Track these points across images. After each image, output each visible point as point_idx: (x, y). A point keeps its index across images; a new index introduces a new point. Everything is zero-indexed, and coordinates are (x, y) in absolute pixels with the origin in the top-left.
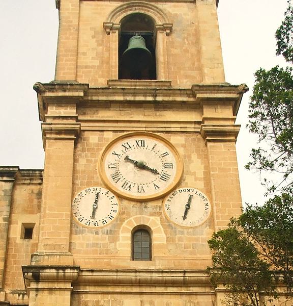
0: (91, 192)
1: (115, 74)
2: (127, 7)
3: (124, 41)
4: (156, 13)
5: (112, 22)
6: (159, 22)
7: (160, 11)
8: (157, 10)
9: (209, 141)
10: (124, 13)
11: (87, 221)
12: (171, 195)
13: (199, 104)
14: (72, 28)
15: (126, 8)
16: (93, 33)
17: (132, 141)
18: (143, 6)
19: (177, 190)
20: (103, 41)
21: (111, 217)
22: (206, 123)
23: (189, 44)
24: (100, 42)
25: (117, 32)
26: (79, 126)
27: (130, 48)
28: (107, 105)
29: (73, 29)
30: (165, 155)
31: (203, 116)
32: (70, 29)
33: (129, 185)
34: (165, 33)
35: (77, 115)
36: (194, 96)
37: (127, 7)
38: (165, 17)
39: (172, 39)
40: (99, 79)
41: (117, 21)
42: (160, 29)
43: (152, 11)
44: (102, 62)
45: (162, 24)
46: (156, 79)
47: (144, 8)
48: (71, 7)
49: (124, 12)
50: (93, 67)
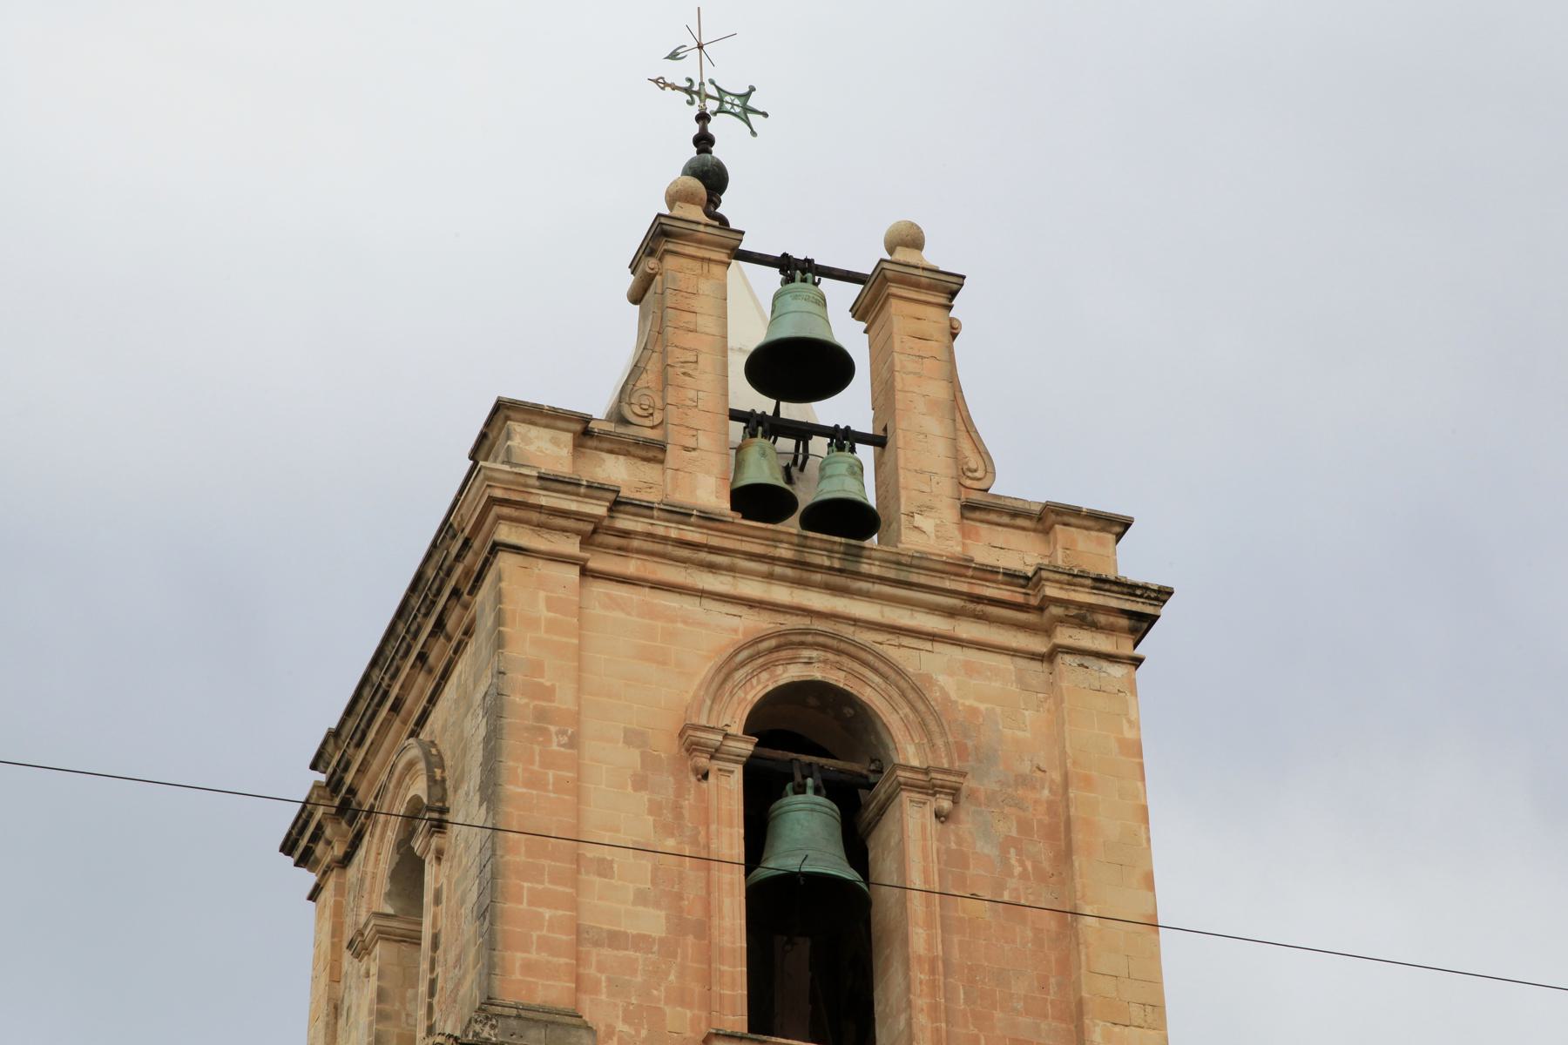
2: (778, 648)
4: (895, 694)
6: (908, 751)
8: (902, 683)
10: (764, 676)
14: (553, 729)
15: (771, 651)
16: (633, 757)
18: (839, 652)
20: (677, 809)
23: (1024, 876)
24: (668, 816)
25: (738, 771)
29: (564, 733)
32: (544, 732)
34: (929, 811)
37: (778, 648)
38: (933, 726)
39: (960, 841)
40: (668, 1010)
43: (877, 679)
44: (679, 925)
47: (844, 660)
48: (544, 613)
49: (764, 668)
50: (641, 942)
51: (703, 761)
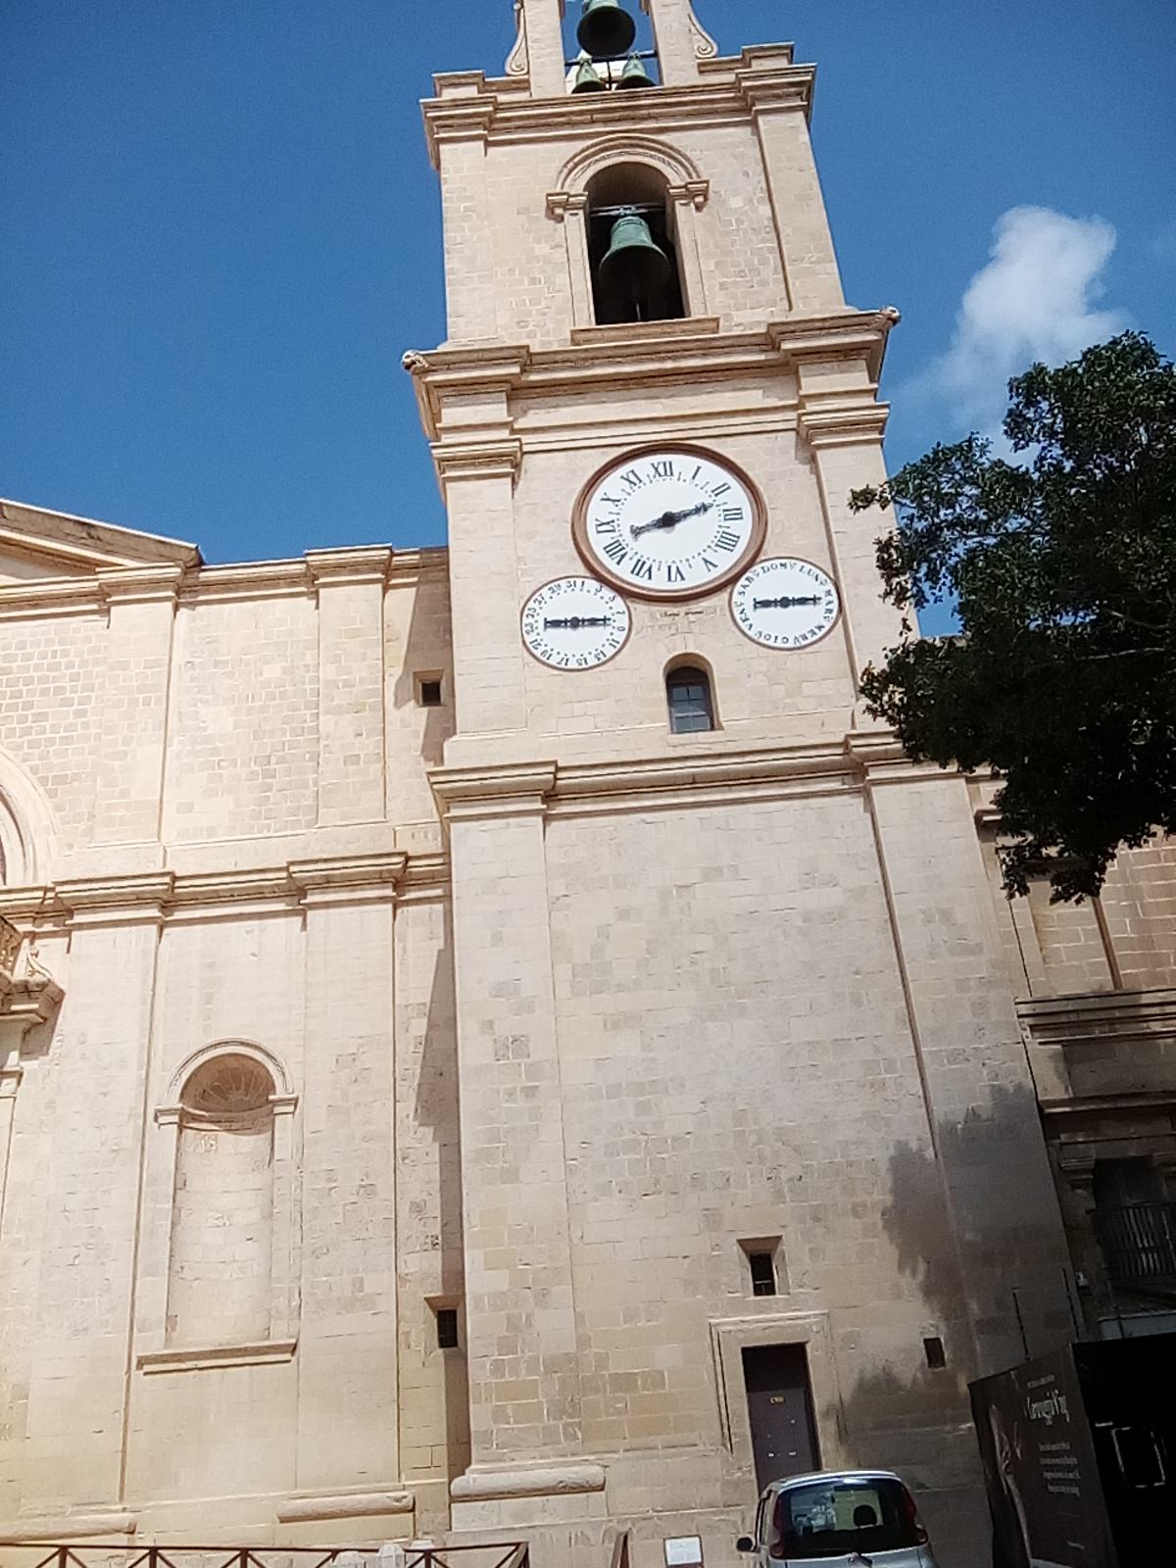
0: (562, 592)
1: (585, 313)
3: (599, 232)
5: (565, 190)
6: (675, 177)
7: (671, 153)
9: (819, 447)
11: (562, 655)
12: (742, 581)
13: (786, 364)
17: (642, 465)
19: (757, 568)
21: (613, 643)
22: (810, 407)
25: (581, 212)
26: (517, 444)
27: (615, 246)
28: (580, 389)
30: (723, 489)
31: (802, 393)
33: (646, 567)
34: (692, 205)
35: (511, 419)
36: (776, 347)
41: (578, 185)
42: (681, 196)
45: (683, 184)
46: (683, 317)
51: (559, 211)
